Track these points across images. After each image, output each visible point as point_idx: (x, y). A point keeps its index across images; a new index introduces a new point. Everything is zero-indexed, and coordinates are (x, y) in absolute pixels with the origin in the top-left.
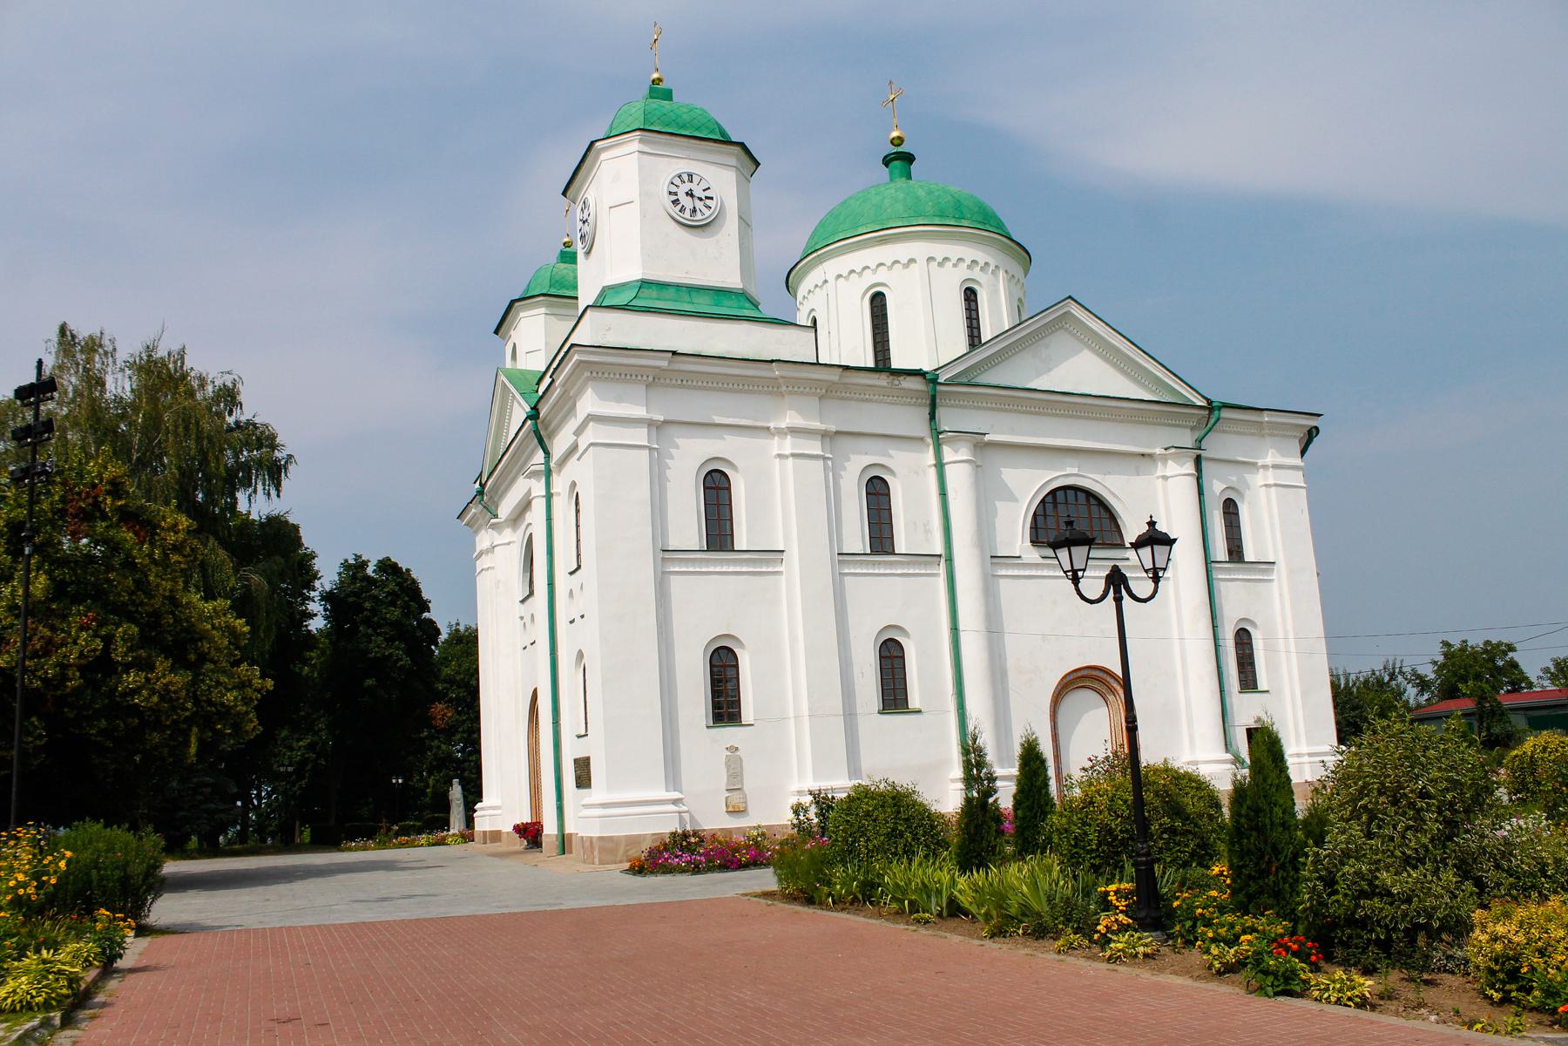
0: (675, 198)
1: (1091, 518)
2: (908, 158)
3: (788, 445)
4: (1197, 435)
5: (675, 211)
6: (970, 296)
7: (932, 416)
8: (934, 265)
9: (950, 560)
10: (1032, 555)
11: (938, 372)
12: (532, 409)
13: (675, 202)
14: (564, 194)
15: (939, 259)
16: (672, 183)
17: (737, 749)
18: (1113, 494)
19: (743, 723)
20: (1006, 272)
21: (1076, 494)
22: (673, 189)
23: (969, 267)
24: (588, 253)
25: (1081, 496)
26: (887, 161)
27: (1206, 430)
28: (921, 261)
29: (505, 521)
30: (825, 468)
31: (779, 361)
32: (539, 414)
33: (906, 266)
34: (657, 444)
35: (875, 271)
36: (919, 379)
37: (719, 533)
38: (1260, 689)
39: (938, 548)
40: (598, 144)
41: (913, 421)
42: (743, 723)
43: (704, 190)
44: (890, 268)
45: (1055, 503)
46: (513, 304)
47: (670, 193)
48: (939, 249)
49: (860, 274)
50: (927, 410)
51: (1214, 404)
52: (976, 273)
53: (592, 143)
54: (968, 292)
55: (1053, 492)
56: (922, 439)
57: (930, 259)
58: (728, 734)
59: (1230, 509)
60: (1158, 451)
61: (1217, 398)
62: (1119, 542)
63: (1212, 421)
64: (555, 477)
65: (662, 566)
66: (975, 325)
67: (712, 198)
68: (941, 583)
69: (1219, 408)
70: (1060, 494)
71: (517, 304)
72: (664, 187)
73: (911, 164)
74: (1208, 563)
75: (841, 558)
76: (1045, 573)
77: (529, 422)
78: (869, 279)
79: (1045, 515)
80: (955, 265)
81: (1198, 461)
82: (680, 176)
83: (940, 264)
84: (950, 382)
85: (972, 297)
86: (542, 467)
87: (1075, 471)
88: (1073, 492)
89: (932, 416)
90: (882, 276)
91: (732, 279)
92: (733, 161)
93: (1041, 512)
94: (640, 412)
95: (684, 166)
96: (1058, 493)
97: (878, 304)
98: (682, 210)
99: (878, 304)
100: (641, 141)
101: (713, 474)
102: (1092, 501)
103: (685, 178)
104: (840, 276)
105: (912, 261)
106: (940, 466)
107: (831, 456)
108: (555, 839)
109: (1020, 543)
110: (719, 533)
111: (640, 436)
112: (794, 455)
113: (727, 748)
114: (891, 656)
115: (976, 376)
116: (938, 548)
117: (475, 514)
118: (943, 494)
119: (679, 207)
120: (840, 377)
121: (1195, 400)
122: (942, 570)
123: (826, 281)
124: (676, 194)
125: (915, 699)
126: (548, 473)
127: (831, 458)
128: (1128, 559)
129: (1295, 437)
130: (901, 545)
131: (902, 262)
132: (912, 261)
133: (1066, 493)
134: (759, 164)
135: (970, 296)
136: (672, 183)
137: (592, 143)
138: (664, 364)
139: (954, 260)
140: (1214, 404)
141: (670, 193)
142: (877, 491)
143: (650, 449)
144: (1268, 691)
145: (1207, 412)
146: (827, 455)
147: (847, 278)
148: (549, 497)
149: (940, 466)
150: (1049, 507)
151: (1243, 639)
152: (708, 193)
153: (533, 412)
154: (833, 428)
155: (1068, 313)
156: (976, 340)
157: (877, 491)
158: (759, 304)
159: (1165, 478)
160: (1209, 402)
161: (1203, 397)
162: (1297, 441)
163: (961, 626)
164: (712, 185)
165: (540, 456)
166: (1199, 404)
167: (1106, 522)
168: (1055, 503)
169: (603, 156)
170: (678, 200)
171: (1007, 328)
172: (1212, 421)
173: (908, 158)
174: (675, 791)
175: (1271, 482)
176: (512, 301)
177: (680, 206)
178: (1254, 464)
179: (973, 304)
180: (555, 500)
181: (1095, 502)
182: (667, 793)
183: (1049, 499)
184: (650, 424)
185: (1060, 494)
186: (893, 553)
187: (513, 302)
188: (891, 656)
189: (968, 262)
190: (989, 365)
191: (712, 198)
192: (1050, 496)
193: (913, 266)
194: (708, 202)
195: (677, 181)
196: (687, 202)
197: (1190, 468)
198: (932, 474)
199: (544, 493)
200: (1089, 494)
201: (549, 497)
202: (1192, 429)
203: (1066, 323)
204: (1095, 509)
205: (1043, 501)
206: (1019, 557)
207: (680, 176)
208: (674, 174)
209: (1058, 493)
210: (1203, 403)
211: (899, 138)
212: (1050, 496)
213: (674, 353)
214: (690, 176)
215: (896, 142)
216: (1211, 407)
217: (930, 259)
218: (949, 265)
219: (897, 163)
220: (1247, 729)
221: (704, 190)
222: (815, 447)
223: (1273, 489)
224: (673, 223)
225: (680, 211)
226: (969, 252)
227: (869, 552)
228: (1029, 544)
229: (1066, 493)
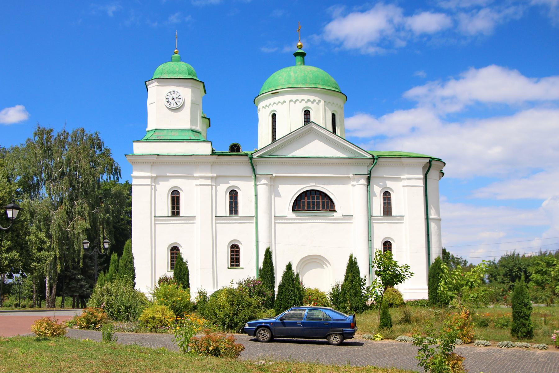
0: (168, 100)
3: (199, 182)
7: (254, 170)
8: (292, 103)
9: (257, 218)
10: (292, 215)
15: (294, 100)
18: (330, 192)
20: (325, 102)
21: (315, 192)
22: (167, 97)
23: (306, 102)
27: (372, 167)
28: (288, 102)
30: (212, 189)
31: (194, 155)
33: (282, 104)
37: (175, 210)
39: (254, 214)
40: (147, 83)
44: (277, 104)
48: (294, 97)
50: (250, 167)
51: (375, 157)
52: (309, 104)
54: (307, 112)
57: (291, 101)
59: (387, 197)
60: (351, 175)
61: (376, 154)
67: (181, 99)
68: (254, 225)
69: (377, 159)
70: (308, 193)
72: (164, 97)
74: (370, 217)
75: (216, 218)
76: (298, 221)
78: (271, 108)
80: (300, 102)
81: (369, 179)
82: (170, 92)
83: (295, 102)
84: (262, 156)
85: (309, 113)
87: (314, 184)
88: (314, 192)
89: (254, 170)
90: (274, 107)
92: (190, 84)
94: (148, 174)
96: (307, 192)
97: (274, 116)
99: (274, 116)
100: (158, 82)
102: (322, 194)
103: (172, 93)
105: (284, 102)
107: (214, 184)
110: (175, 210)
111: (148, 181)
114: (235, 250)
116: (254, 214)
118: (256, 196)
119: (169, 103)
122: (254, 221)
125: (242, 263)
130: (240, 213)
131: (281, 104)
132: (284, 102)
138: (155, 159)
139: (300, 100)
140: (375, 157)
141: (166, 99)
142: (233, 196)
143: (151, 185)
146: (213, 184)
149: (256, 186)
152: (180, 97)
154: (215, 175)
155: (312, 127)
157: (233, 196)
159: (354, 186)
160: (372, 155)
161: (371, 154)
163: (259, 241)
164: (181, 94)
166: (369, 157)
172: (374, 163)
175: (405, 184)
177: (169, 103)
178: (400, 178)
181: (324, 195)
184: (151, 178)
188: (235, 250)
189: (306, 100)
191: (181, 99)
193: (284, 104)
194: (180, 100)
195: (169, 94)
196: (173, 102)
197: (364, 181)
198: (253, 188)
202: (368, 166)
205: (300, 195)
206: (286, 216)
209: (307, 192)
210: (371, 157)
211: (300, 46)
212: (304, 194)
213: (158, 155)
214: (174, 92)
216: (374, 158)
217: (291, 101)
218: (298, 102)
222: (208, 182)
223: (406, 188)
226: (306, 97)
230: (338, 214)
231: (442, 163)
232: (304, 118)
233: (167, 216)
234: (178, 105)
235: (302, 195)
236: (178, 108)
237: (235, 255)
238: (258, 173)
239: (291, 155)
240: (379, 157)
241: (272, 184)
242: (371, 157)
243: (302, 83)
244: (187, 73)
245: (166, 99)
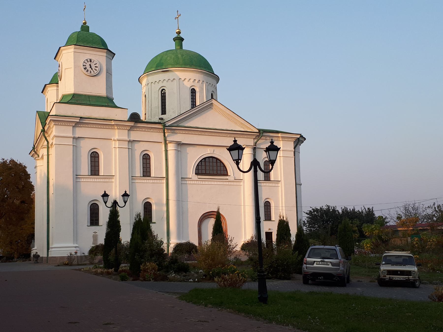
0: (85, 67)
1: (217, 166)
2: (182, 39)
4: (256, 140)
5: (85, 71)
6: (193, 92)
10: (196, 177)
11: (165, 123)
12: (43, 128)
13: (85, 68)
14: (55, 59)
16: (84, 62)
17: (97, 232)
19: (100, 225)
22: (85, 64)
23: (193, 82)
24: (60, 80)
25: (215, 160)
26: (175, 39)
29: (41, 158)
32: (45, 130)
33: (172, 81)
34: (76, 144)
35: (163, 82)
36: (161, 125)
38: (272, 220)
40: (61, 48)
41: (159, 137)
42: (100, 225)
43: (95, 64)
44: (167, 81)
45: (205, 162)
46: (46, 86)
47: (84, 65)
49: (158, 83)
53: (60, 48)
54: (193, 90)
55: (205, 159)
58: (94, 228)
62: (225, 173)
63: (260, 137)
64: (50, 149)
65: (76, 180)
66: (194, 101)
67: (97, 67)
68: (165, 185)
70: (207, 159)
71: (47, 86)
73: (183, 41)
77: (42, 133)
78: (161, 84)
79: (201, 165)
86: (46, 146)
91: (102, 92)
93: (200, 164)
95: (88, 57)
96: (206, 159)
98: (88, 71)
101: (94, 153)
102: (218, 161)
103: (89, 60)
104: (152, 82)
106: (166, 151)
109: (192, 174)
112: (118, 148)
113: (94, 232)
115: (180, 124)
117: (33, 154)
119: (86, 70)
120: (134, 124)
121: (255, 130)
122: (164, 181)
123: (148, 84)
124: (85, 66)
126: (48, 148)
127: (131, 149)
128: (228, 179)
129: (292, 141)
130: (153, 174)
133: (209, 158)
134: (115, 54)
135: (193, 92)
136: (84, 62)
137: (60, 48)
138: (78, 121)
143: (73, 146)
144: (274, 221)
145: (258, 134)
147: (154, 84)
148: (48, 155)
149: (166, 151)
150: (203, 163)
151: (267, 205)
153: (44, 130)
156: (194, 106)
157: (146, 159)
158: (113, 100)
161: (257, 129)
162: (293, 142)
165: (46, 142)
167: (222, 168)
168: (205, 162)
169: (64, 52)
170: (86, 68)
171: (205, 101)
173: (182, 39)
174: (76, 244)
176: (45, 85)
179: (194, 94)
180: (50, 156)
181: (220, 162)
182: (74, 245)
183: (204, 160)
185: (207, 159)
186: (150, 176)
187: (45, 85)
190: (186, 119)
191: (97, 67)
192: (204, 160)
193: (175, 81)
195: (86, 62)
199: (47, 154)
200: (217, 159)
201: (48, 155)
203: (212, 106)
204: (219, 164)
206: (191, 178)
207: (87, 60)
208: (85, 59)
209: (206, 159)
210: (257, 131)
211: (179, 32)
212: (204, 160)
213: (81, 118)
215: (178, 33)
219: (177, 41)
220: (266, 232)
221: (95, 64)
224: (85, 75)
225: (87, 71)
227: (142, 176)
228: (195, 174)
229: (209, 158)
230: (231, 178)
231: (303, 138)
232: (195, 96)
233: (87, 175)
234: (95, 72)
235: (202, 161)
236: (97, 74)
237: (148, 212)
238: (168, 140)
239: (186, 125)
240: (264, 132)
241: (179, 150)
242: (257, 131)
243: (189, 65)
244: (101, 43)
245: (84, 65)
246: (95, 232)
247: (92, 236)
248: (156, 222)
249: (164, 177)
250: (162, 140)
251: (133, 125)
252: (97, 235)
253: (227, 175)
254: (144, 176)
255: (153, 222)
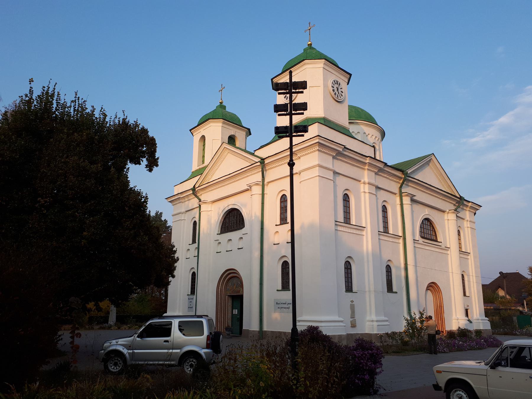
7: (401, 187)
39: (400, 234)
41: (394, 187)
42: (353, 291)
56: (395, 194)
64: (266, 187)
106: (402, 205)
108: (257, 333)
149: (402, 205)
165: (258, 177)
199: (261, 193)
246: (352, 301)
247: (349, 306)
248: (398, 292)
249: (401, 235)
250: (397, 191)
251: (382, 167)
252: (354, 305)
253: (436, 241)
254: (384, 232)
255: (393, 291)
